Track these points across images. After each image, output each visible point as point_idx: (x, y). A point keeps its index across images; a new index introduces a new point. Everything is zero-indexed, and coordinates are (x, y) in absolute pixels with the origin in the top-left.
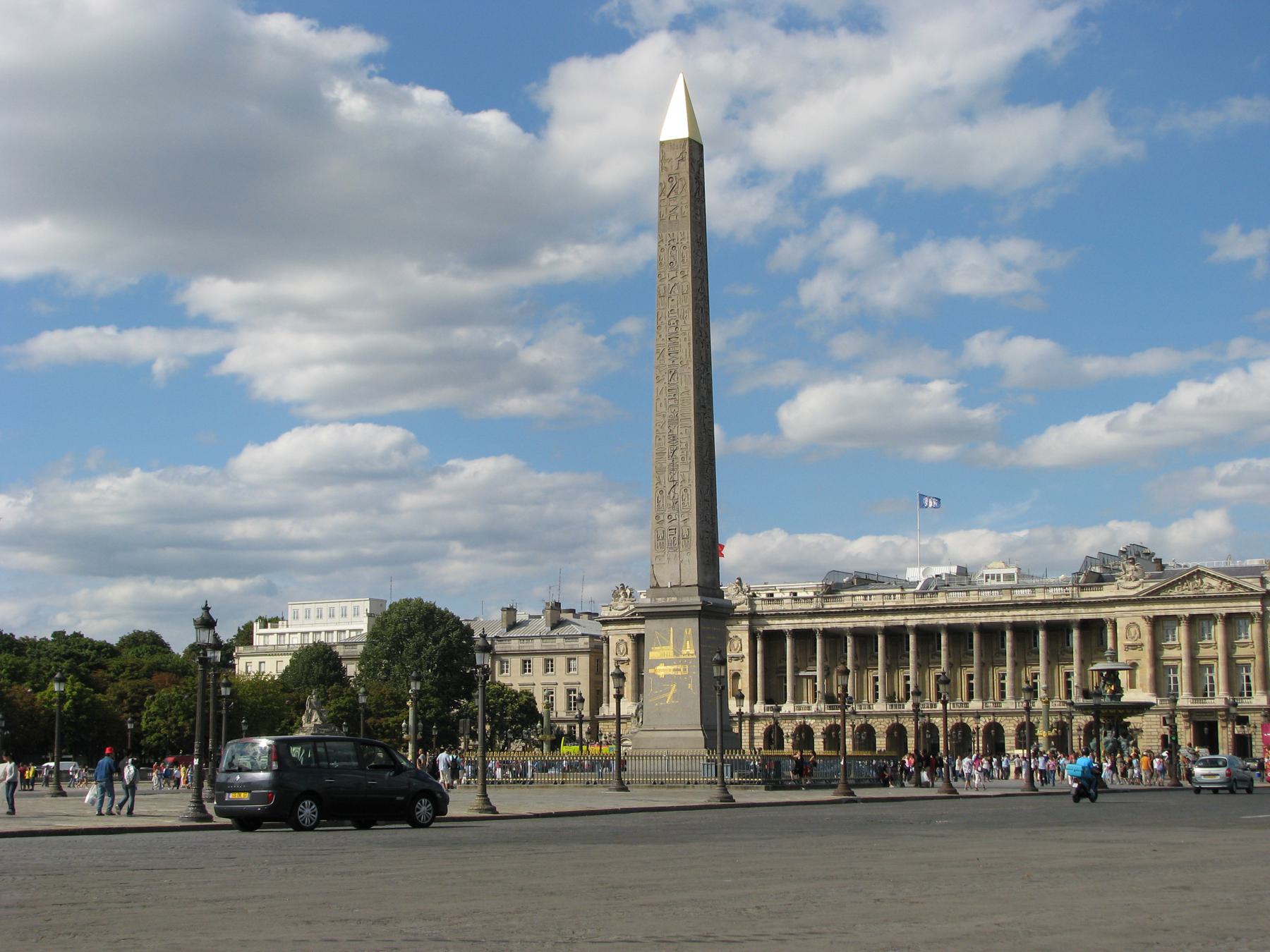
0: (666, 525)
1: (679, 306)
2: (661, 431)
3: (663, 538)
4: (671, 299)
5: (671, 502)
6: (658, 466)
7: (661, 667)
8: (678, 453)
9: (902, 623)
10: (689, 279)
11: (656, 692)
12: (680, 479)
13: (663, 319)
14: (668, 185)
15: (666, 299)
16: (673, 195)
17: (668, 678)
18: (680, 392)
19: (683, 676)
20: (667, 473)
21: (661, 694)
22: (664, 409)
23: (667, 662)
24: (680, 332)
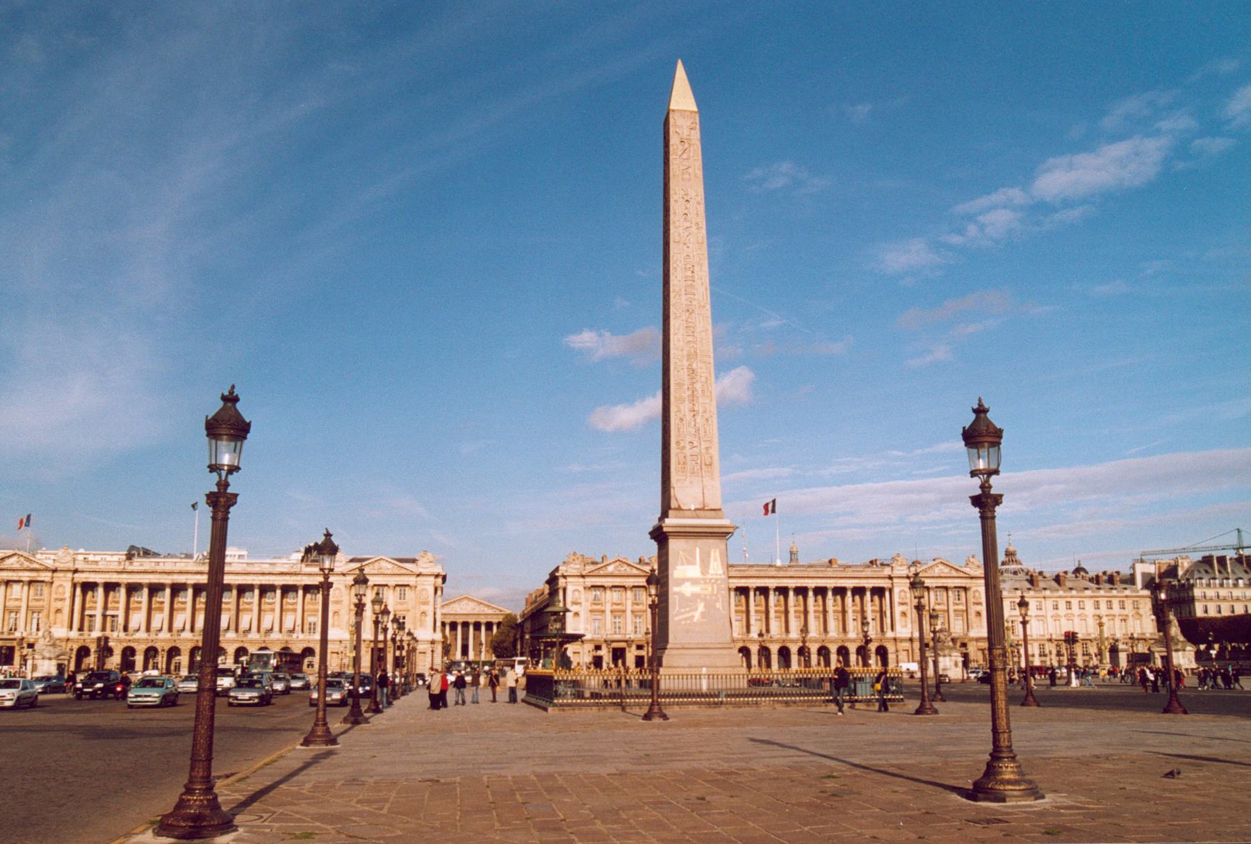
0: (688, 452)
1: (695, 253)
2: (679, 363)
3: (684, 463)
4: (685, 247)
5: (692, 430)
6: (678, 395)
7: (688, 584)
8: (698, 386)
9: (183, 581)
10: (704, 231)
11: (683, 610)
12: (701, 410)
13: (678, 263)
14: (681, 148)
15: (681, 245)
16: (685, 156)
17: (695, 597)
19: (712, 595)
20: (687, 403)
21: (688, 612)
22: (681, 344)
23: (694, 581)
24: (696, 277)
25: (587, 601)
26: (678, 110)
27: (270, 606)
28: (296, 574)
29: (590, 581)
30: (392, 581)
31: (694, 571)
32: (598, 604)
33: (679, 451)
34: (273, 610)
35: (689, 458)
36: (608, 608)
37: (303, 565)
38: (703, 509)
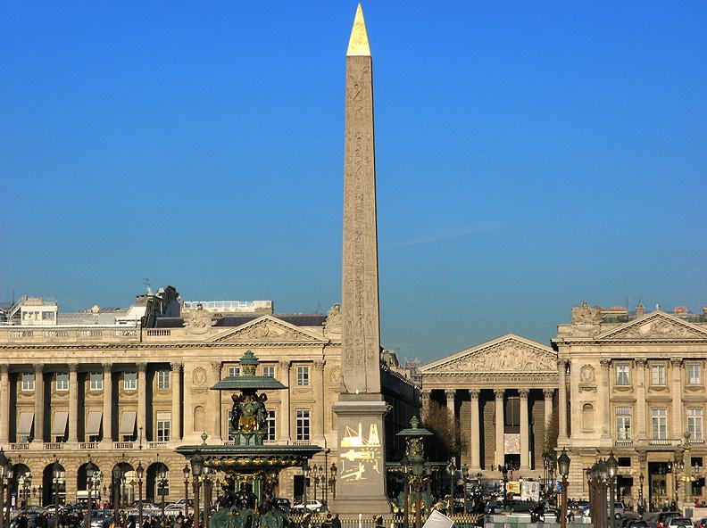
0: (354, 348)
2: (349, 277)
7: (352, 451)
8: (364, 294)
14: (355, 91)
16: (358, 98)
17: (358, 461)
18: (366, 248)
23: (357, 449)
24: (365, 204)
25: (606, 384)
26: (353, 57)
27: (96, 398)
28: (133, 346)
29: (609, 351)
30: (285, 355)
31: (356, 441)
32: (627, 389)
33: (348, 347)
34: (101, 403)
35: (355, 351)
36: (640, 395)
37: (144, 332)
38: (365, 393)
